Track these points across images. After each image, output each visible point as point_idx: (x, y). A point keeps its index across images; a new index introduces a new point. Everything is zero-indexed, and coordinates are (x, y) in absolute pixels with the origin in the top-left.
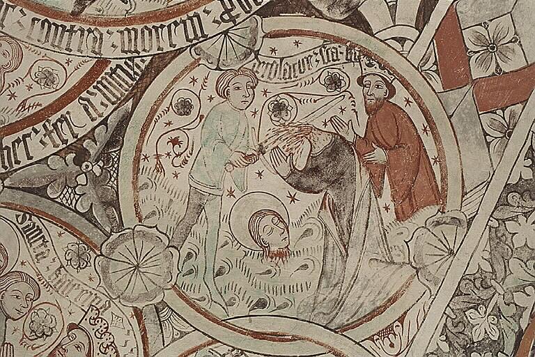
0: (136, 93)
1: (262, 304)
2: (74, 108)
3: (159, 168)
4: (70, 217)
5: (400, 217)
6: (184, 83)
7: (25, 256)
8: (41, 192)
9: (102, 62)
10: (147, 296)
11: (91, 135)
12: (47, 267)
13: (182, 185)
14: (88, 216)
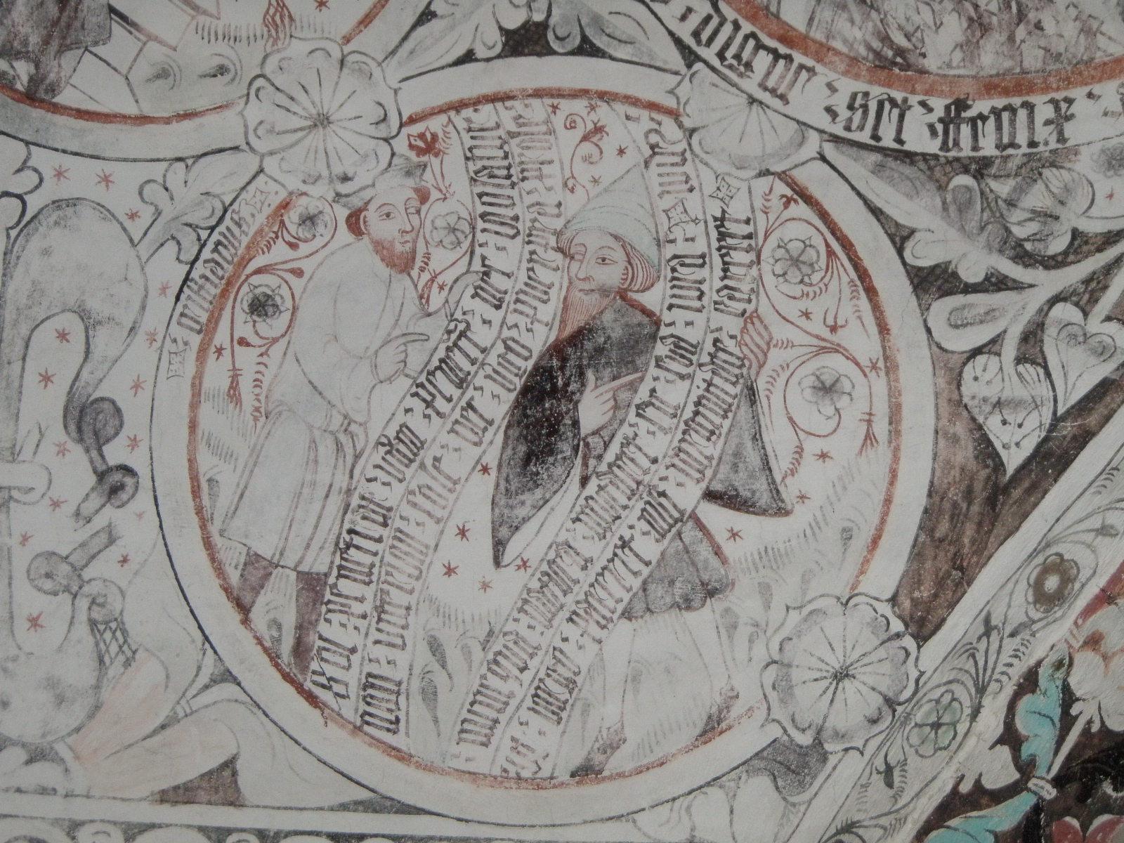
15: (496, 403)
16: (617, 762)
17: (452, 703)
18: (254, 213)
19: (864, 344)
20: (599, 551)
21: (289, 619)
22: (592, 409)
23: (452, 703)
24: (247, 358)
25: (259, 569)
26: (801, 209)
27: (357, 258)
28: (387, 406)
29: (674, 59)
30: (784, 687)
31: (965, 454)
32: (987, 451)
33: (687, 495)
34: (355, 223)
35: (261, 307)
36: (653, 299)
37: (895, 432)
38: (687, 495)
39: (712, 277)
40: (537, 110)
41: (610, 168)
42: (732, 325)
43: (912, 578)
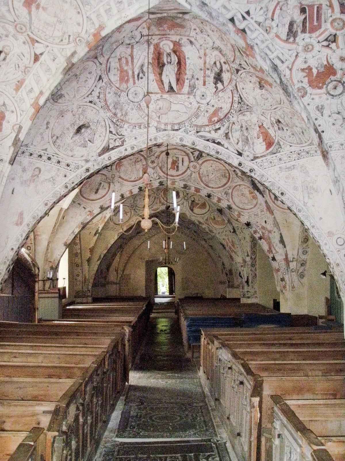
0: (237, 91)
1: (271, 106)
2: (234, 98)
3: (248, 98)
4: (246, 110)
5: (272, 88)
6: (240, 86)
8: (241, 110)
9: (232, 90)
10: (261, 112)
11: (239, 100)
12: (249, 117)
13: (252, 98)
15: (76, 127)
16: (75, 156)
17: (64, 148)
19: (104, 135)
20: (79, 141)
22: (83, 130)
23: (64, 148)
24: (60, 120)
25: (54, 135)
30: (88, 155)
31: (107, 145)
32: (109, 146)
34: (72, 112)
35: (62, 116)
36: (90, 124)
38: (87, 139)
40: (89, 107)
42: (95, 128)
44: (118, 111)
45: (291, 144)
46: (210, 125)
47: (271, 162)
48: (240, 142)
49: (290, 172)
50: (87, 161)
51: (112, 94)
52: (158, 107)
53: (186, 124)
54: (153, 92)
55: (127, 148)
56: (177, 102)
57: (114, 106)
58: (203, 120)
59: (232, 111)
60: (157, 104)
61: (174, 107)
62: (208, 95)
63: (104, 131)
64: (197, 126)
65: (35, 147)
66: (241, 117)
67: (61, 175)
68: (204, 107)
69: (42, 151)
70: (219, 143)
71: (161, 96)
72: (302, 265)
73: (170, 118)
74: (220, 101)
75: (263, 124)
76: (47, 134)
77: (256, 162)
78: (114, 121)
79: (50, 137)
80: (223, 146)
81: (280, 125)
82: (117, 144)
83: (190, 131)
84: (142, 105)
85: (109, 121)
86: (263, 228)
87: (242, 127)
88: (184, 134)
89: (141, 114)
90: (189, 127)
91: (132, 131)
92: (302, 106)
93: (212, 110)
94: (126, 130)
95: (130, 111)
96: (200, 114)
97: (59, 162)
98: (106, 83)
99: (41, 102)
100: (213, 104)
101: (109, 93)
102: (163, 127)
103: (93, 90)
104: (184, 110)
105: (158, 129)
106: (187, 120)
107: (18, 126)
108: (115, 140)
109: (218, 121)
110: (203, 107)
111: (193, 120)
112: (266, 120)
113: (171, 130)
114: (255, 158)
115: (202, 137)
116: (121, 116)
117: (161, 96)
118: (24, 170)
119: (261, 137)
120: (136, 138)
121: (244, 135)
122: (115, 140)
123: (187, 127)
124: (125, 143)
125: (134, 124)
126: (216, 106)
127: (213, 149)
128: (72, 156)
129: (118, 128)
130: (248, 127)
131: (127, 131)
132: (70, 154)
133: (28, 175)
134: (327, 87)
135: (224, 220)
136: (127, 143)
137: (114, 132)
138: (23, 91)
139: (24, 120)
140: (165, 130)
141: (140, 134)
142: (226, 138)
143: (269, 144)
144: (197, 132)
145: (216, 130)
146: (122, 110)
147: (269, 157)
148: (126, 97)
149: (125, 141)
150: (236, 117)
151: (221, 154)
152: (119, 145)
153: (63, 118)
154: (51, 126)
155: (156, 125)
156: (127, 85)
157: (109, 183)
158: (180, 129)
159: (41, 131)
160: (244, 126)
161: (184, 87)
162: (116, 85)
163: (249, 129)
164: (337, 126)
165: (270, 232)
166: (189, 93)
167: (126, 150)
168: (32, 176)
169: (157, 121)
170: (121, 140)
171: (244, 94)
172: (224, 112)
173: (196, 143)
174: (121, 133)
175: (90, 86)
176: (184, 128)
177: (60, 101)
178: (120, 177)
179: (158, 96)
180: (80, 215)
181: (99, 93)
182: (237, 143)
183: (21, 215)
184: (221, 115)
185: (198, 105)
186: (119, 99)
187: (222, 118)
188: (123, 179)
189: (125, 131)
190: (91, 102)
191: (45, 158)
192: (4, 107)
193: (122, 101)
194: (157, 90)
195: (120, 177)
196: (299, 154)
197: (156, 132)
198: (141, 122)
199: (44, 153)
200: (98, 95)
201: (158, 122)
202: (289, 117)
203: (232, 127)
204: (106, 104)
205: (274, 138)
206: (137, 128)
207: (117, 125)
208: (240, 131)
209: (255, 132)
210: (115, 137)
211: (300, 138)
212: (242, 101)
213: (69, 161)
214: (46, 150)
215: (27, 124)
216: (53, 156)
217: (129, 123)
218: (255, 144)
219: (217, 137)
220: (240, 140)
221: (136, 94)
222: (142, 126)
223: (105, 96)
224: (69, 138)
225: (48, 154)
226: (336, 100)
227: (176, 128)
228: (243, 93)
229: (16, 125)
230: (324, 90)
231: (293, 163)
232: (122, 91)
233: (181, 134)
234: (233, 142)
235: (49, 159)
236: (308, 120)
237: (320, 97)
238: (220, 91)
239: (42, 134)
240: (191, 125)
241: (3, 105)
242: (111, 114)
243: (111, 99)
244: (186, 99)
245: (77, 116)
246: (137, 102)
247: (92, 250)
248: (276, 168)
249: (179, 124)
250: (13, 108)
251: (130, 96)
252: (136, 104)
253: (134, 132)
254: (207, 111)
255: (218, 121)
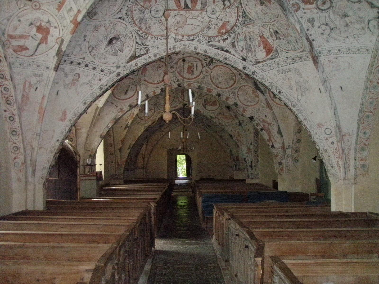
0: (242, 7)
1: (270, 19)
2: (239, 13)
3: (251, 12)
5: (270, 4)
7: (249, 29)
8: (244, 23)
10: (262, 24)
11: (243, 15)
13: (253, 13)
14: (250, 22)
15: (108, 40)
16: (107, 63)
17: (99, 57)
18: (99, 25)
19: (131, 44)
20: (111, 51)
21: (91, 50)
22: (114, 42)
23: (99, 57)
25: (90, 46)
26: (131, 35)
27: (104, 29)
28: (102, 38)
29: (128, 22)
30: (119, 63)
31: (134, 54)
32: (136, 54)
33: (117, 49)
34: (105, 26)
35: (97, 30)
36: (120, 36)
37: (131, 51)
38: (117, 49)
39: (124, 36)
41: (121, 28)
43: (128, 60)
44: (143, 25)
45: (287, 51)
46: (219, 36)
47: (270, 66)
48: (245, 49)
49: (286, 74)
50: (118, 67)
51: (137, 11)
52: (176, 22)
53: (200, 36)
54: (171, 9)
55: (151, 56)
56: (191, 17)
57: (139, 21)
58: (213, 32)
59: (237, 24)
60: (175, 19)
61: (189, 21)
62: (217, 10)
63: (132, 42)
64: (208, 36)
65: (75, 56)
66: (245, 29)
67: (96, 79)
68: (214, 21)
69: (81, 60)
70: (227, 51)
71: (179, 12)
72: (296, 151)
73: (187, 30)
74: (228, 16)
75: (263, 35)
76: (85, 46)
77: (258, 66)
78: (140, 33)
79: (87, 47)
80: (230, 53)
81: (278, 36)
82: (142, 53)
83: (203, 41)
84: (162, 20)
85: (136, 34)
86: (264, 121)
87: (246, 37)
88: (198, 43)
89: (162, 27)
90: (202, 38)
91: (154, 42)
92: (296, 19)
93: (220, 23)
94: (150, 41)
95: (153, 25)
96: (211, 27)
97: (95, 68)
98: (132, 2)
99: (79, 18)
100: (221, 18)
101: (135, 10)
102: (180, 38)
103: (122, 9)
104: (198, 24)
105: (176, 40)
106: (200, 32)
107: (60, 39)
108: (141, 49)
109: (226, 33)
110: (213, 21)
111: (205, 31)
112: (266, 31)
113: (187, 41)
114: (257, 63)
115: (212, 45)
116: (145, 29)
117: (179, 12)
118: (66, 76)
119: (262, 46)
120: (158, 48)
121: (247, 44)
122: (141, 49)
123: (200, 38)
124: (149, 52)
125: (156, 36)
126: (224, 20)
127: (222, 56)
128: (105, 63)
129: (143, 39)
130: (251, 37)
131: (151, 42)
132: (104, 61)
133: (69, 80)
134: (317, 3)
135: (231, 116)
136: (150, 51)
137: (140, 43)
138: (64, 10)
139: (65, 35)
140: (182, 40)
141: (160, 44)
142: (233, 47)
143: (269, 50)
144: (209, 42)
145: (224, 40)
146: (146, 24)
147: (268, 62)
148: (149, 13)
149: (149, 50)
150: (241, 29)
151: (228, 60)
152: (144, 53)
153: (97, 32)
154: (87, 38)
155: (174, 36)
156: (150, 3)
157: (136, 86)
158: (194, 39)
159: (80, 43)
160: (247, 36)
161: (197, 4)
162: (141, 3)
163: (252, 39)
164: (326, 36)
165: (269, 124)
166: (201, 10)
167: (150, 57)
168: (73, 80)
169: (175, 33)
170: (145, 49)
171: (247, 10)
172: (231, 25)
173: (207, 51)
174: (146, 43)
175: (119, 5)
176: (198, 39)
177: (95, 18)
178: (145, 81)
179: (176, 12)
180: (113, 112)
181: (127, 11)
182: (242, 51)
183: (65, 112)
184: (228, 27)
185: (209, 20)
186: (143, 15)
187: (229, 29)
188: (147, 82)
189: (148, 42)
190: (120, 18)
191: (83, 65)
192: (48, 24)
193: (146, 17)
194: (175, 7)
195: (145, 81)
196: (293, 59)
197: (174, 42)
198: (162, 34)
199: (83, 61)
200: (126, 12)
201: (176, 34)
202: (285, 28)
203: (237, 37)
204: (133, 19)
205: (273, 46)
206: (159, 39)
207: (142, 37)
208: (244, 40)
209: (256, 42)
210: (140, 47)
211: (294, 46)
212: (246, 15)
213: (103, 67)
214: (84, 58)
215: (68, 38)
216: (90, 63)
217: (152, 35)
218: (257, 51)
219: (226, 46)
220: (244, 48)
221: (157, 11)
222: (163, 38)
223: (132, 13)
224: (102, 48)
225: (85, 62)
226: (325, 14)
227: (191, 38)
228: (247, 9)
229: (59, 38)
230: (314, 6)
231: (288, 67)
232: (146, 9)
233: (195, 43)
234: (238, 50)
235: (87, 66)
236: (301, 30)
237: (311, 12)
238: (227, 8)
239: (80, 45)
240: (204, 36)
241: (48, 22)
242: (137, 28)
243: (136, 15)
244: (199, 15)
245: (109, 30)
246: (159, 18)
247: (123, 141)
248: (275, 71)
249: (193, 35)
250: (56, 25)
251: (153, 13)
252: (157, 19)
253: (156, 43)
254: (217, 24)
255: (226, 33)
